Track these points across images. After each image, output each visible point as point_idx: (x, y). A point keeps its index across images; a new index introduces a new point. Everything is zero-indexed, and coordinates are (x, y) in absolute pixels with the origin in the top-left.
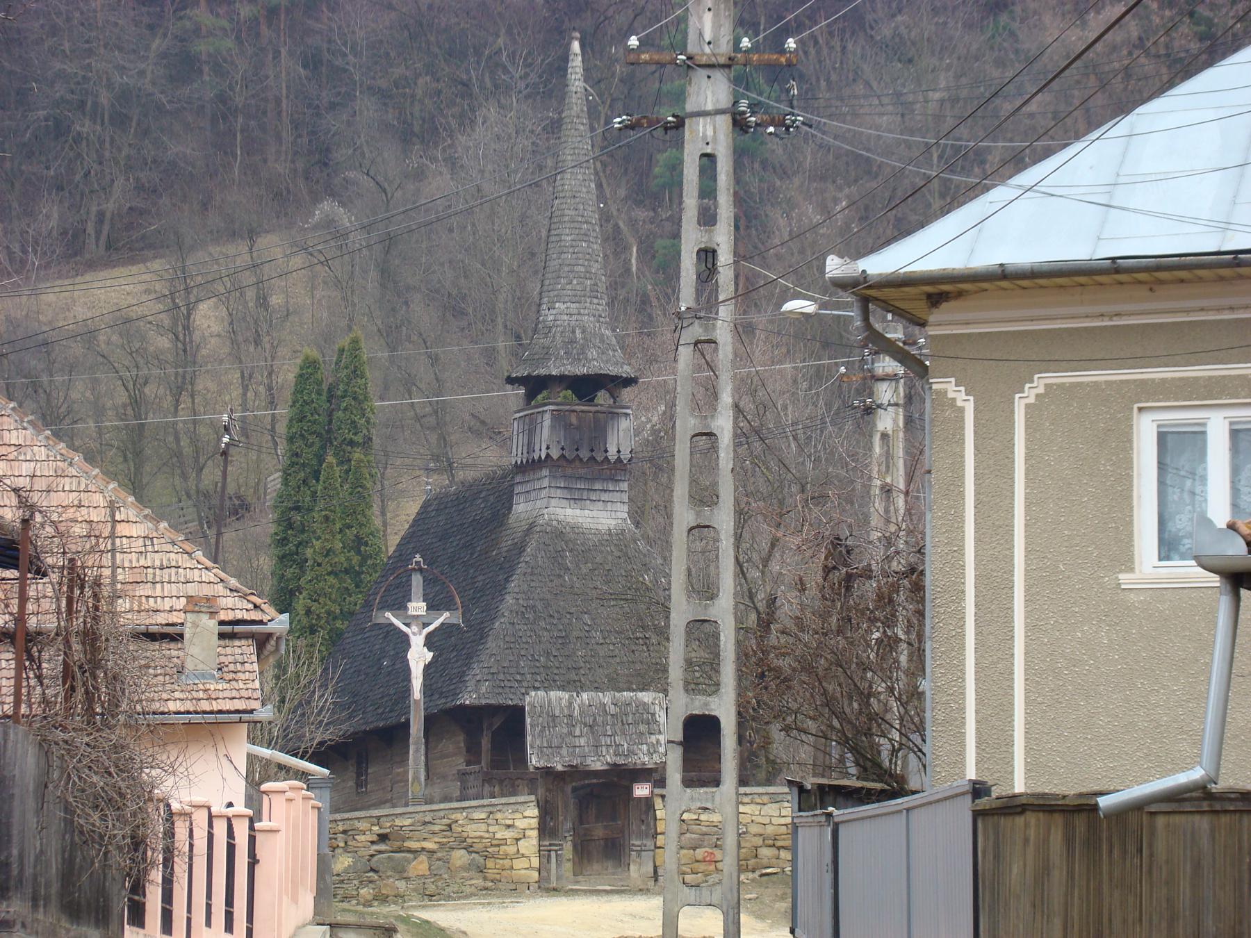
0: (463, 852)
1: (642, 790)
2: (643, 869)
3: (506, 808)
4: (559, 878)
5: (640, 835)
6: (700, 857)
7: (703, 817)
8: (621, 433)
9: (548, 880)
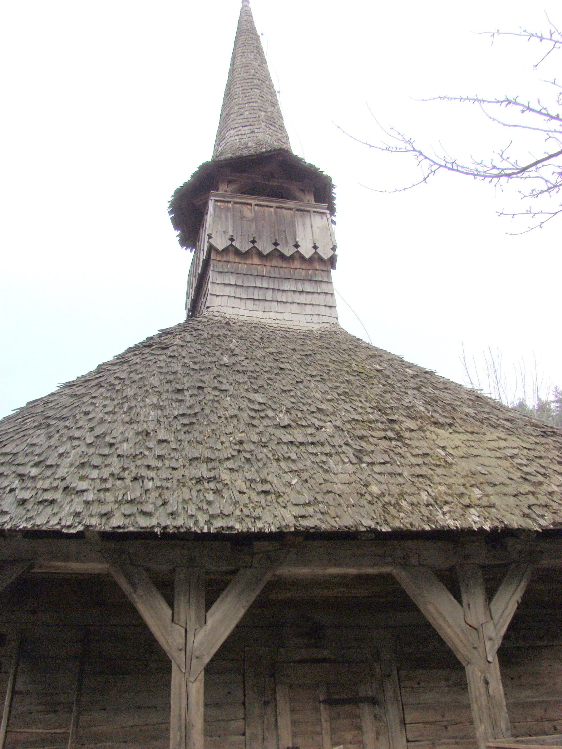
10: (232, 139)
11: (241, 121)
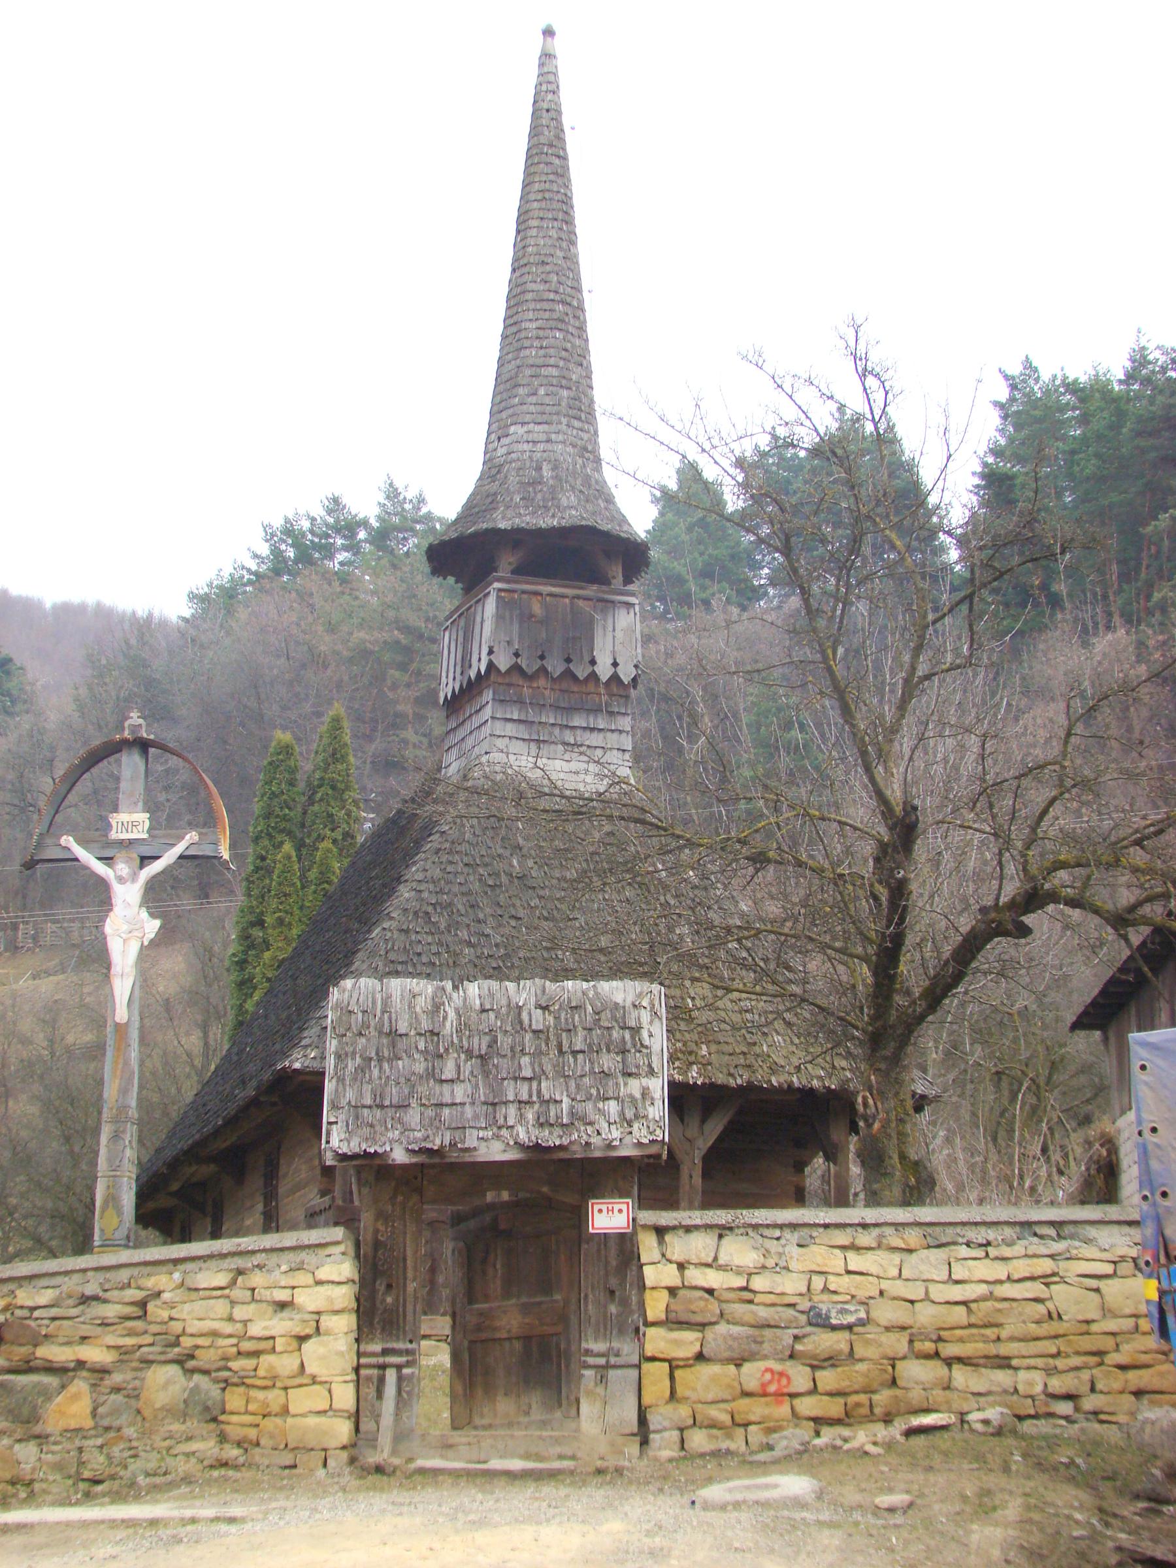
0: (173, 1370)
2: (613, 1415)
3: (274, 1259)
4: (400, 1437)
5: (605, 1327)
6: (752, 1385)
7: (758, 1283)
8: (619, 634)
9: (373, 1442)
10: (521, 447)
11: (532, 408)
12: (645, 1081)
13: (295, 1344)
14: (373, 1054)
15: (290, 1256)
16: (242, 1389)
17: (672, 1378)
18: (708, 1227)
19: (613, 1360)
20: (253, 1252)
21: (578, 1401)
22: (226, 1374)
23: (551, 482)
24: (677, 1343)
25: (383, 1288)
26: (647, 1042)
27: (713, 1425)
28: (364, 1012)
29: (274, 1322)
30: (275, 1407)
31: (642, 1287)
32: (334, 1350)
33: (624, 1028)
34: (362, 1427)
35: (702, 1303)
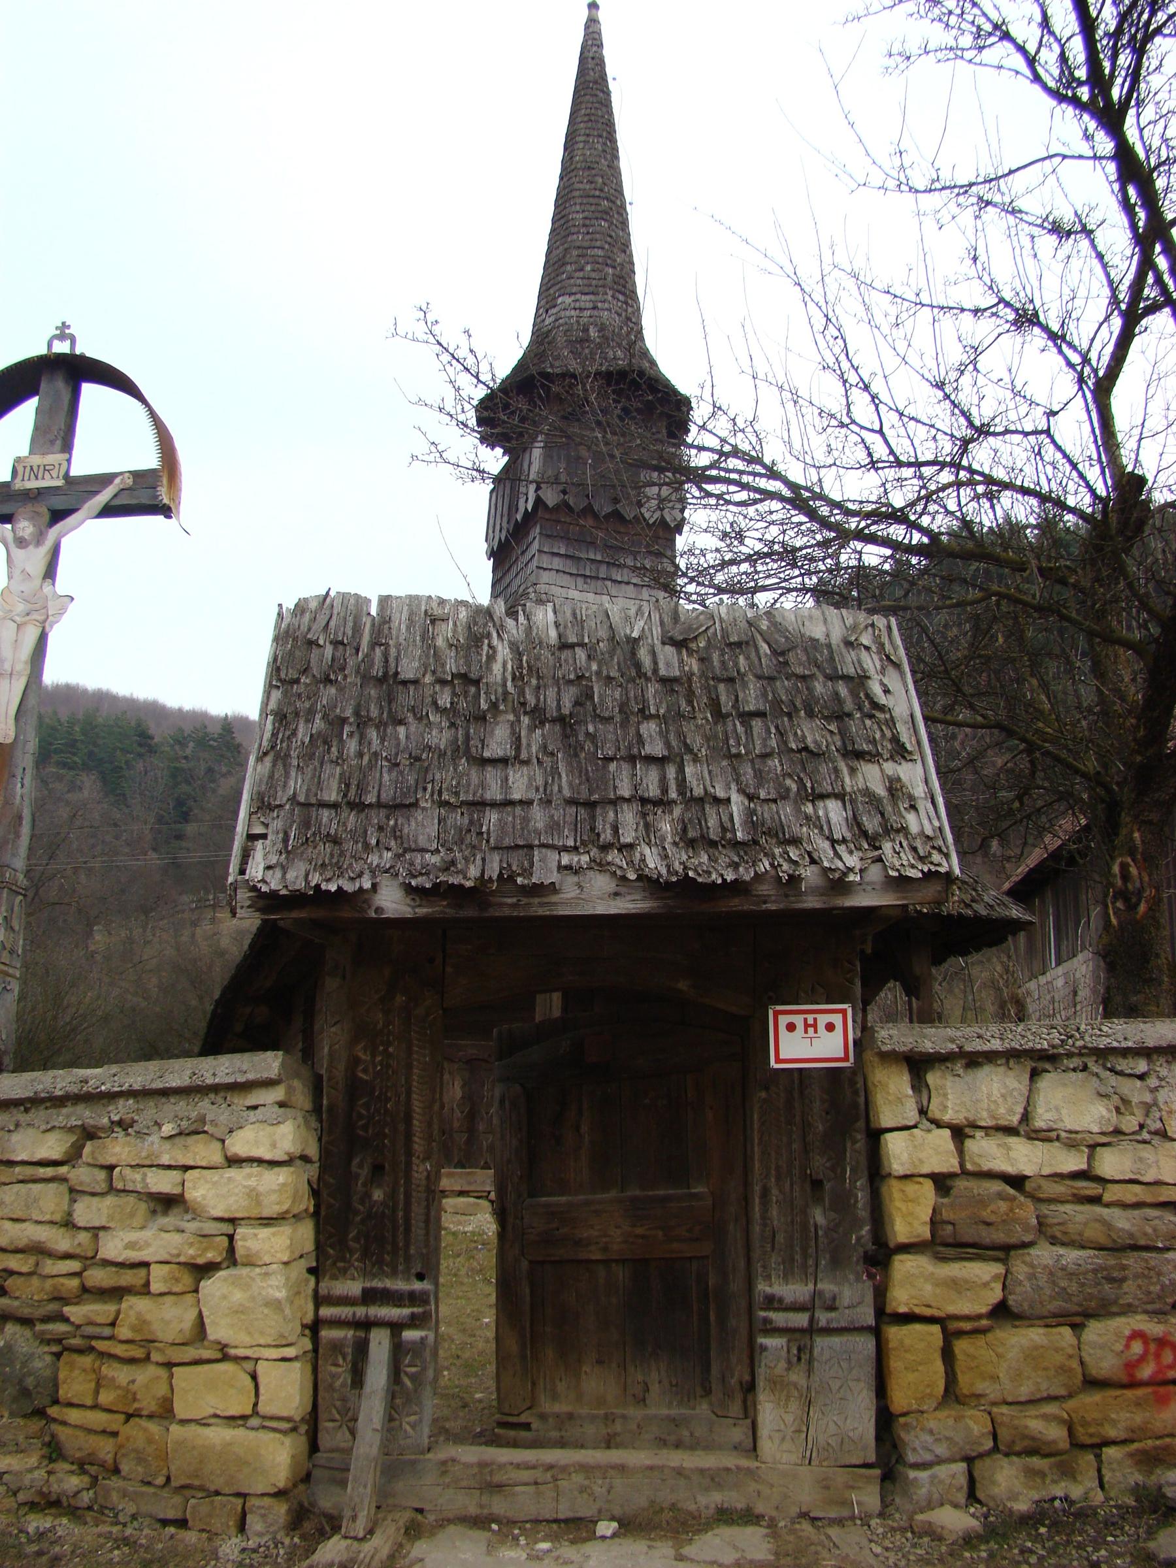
1: (808, 1040)
3: (149, 1111)
6: (1106, 1365)
7: (1111, 1164)
10: (568, 313)
11: (579, 282)
12: (889, 767)
13: (187, 1280)
14: (348, 713)
15: (180, 1106)
16: (87, 1361)
17: (947, 1354)
18: (1012, 1056)
19: (823, 1318)
20: (111, 1096)
21: (750, 1388)
22: (60, 1328)
23: (598, 340)
24: (955, 1284)
25: (364, 1172)
26: (882, 699)
27: (1035, 1448)
28: (337, 643)
29: (147, 1234)
30: (148, 1404)
31: (876, 1171)
32: (262, 1297)
33: (834, 677)
34: (325, 1441)
35: (1003, 1206)
